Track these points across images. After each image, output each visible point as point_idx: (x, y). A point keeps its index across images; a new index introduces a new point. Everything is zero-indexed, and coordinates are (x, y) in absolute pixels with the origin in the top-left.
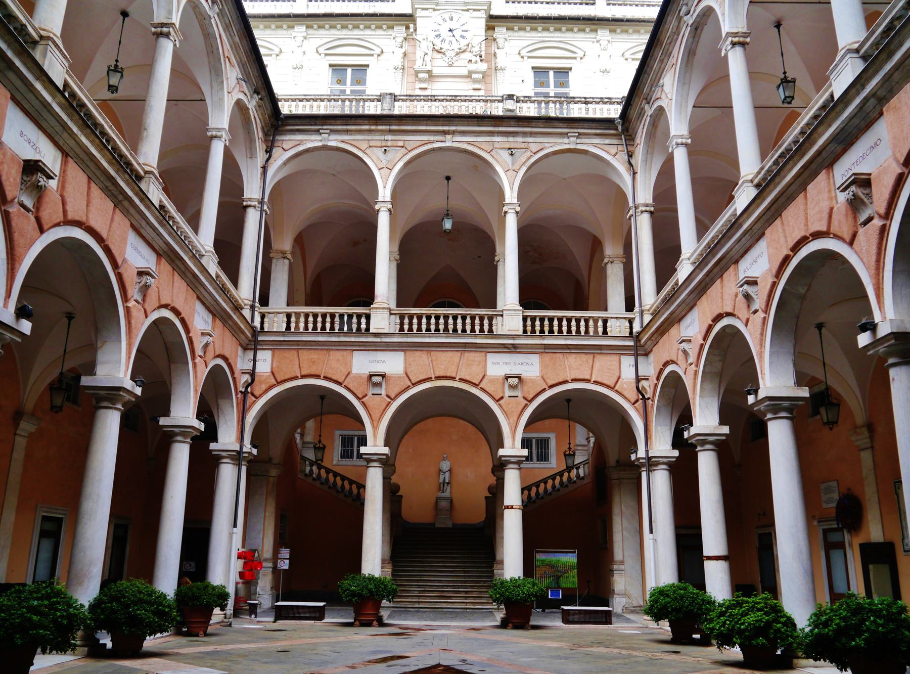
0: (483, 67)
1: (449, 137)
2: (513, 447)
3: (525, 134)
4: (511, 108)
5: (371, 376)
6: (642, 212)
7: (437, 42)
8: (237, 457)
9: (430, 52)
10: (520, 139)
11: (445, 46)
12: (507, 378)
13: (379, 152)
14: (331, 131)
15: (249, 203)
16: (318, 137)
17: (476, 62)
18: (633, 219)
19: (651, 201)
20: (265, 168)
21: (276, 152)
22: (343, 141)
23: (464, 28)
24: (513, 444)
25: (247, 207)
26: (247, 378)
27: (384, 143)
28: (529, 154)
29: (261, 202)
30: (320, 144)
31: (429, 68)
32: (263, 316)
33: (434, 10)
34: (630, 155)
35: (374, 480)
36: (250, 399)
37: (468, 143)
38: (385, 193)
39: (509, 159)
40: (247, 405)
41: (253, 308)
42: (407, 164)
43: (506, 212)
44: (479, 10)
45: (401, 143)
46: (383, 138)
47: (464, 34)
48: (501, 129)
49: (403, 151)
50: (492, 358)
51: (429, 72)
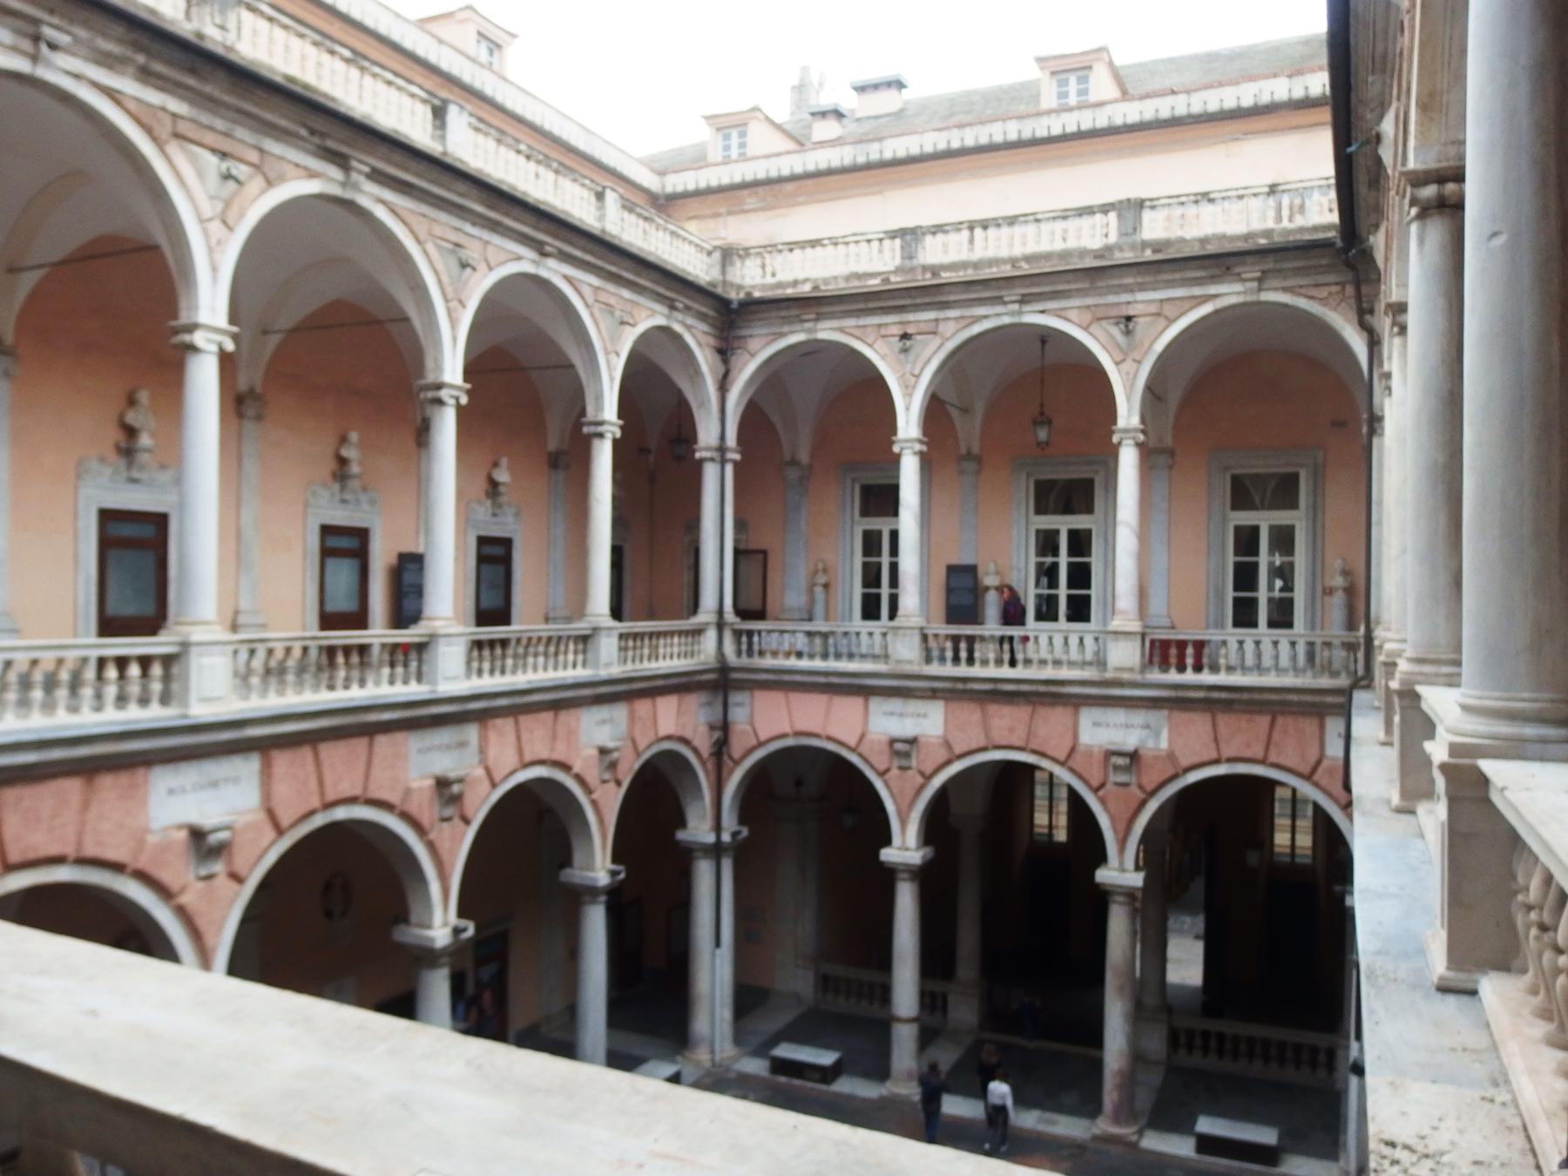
2: (1123, 870)
5: (893, 741)
8: (716, 851)
12: (1110, 753)
20: (723, 388)
24: (1121, 863)
25: (702, 461)
26: (717, 734)
29: (722, 449)
32: (738, 634)
35: (906, 902)
36: (728, 762)
40: (725, 774)
41: (720, 626)
43: (1120, 443)
50: (1087, 717)
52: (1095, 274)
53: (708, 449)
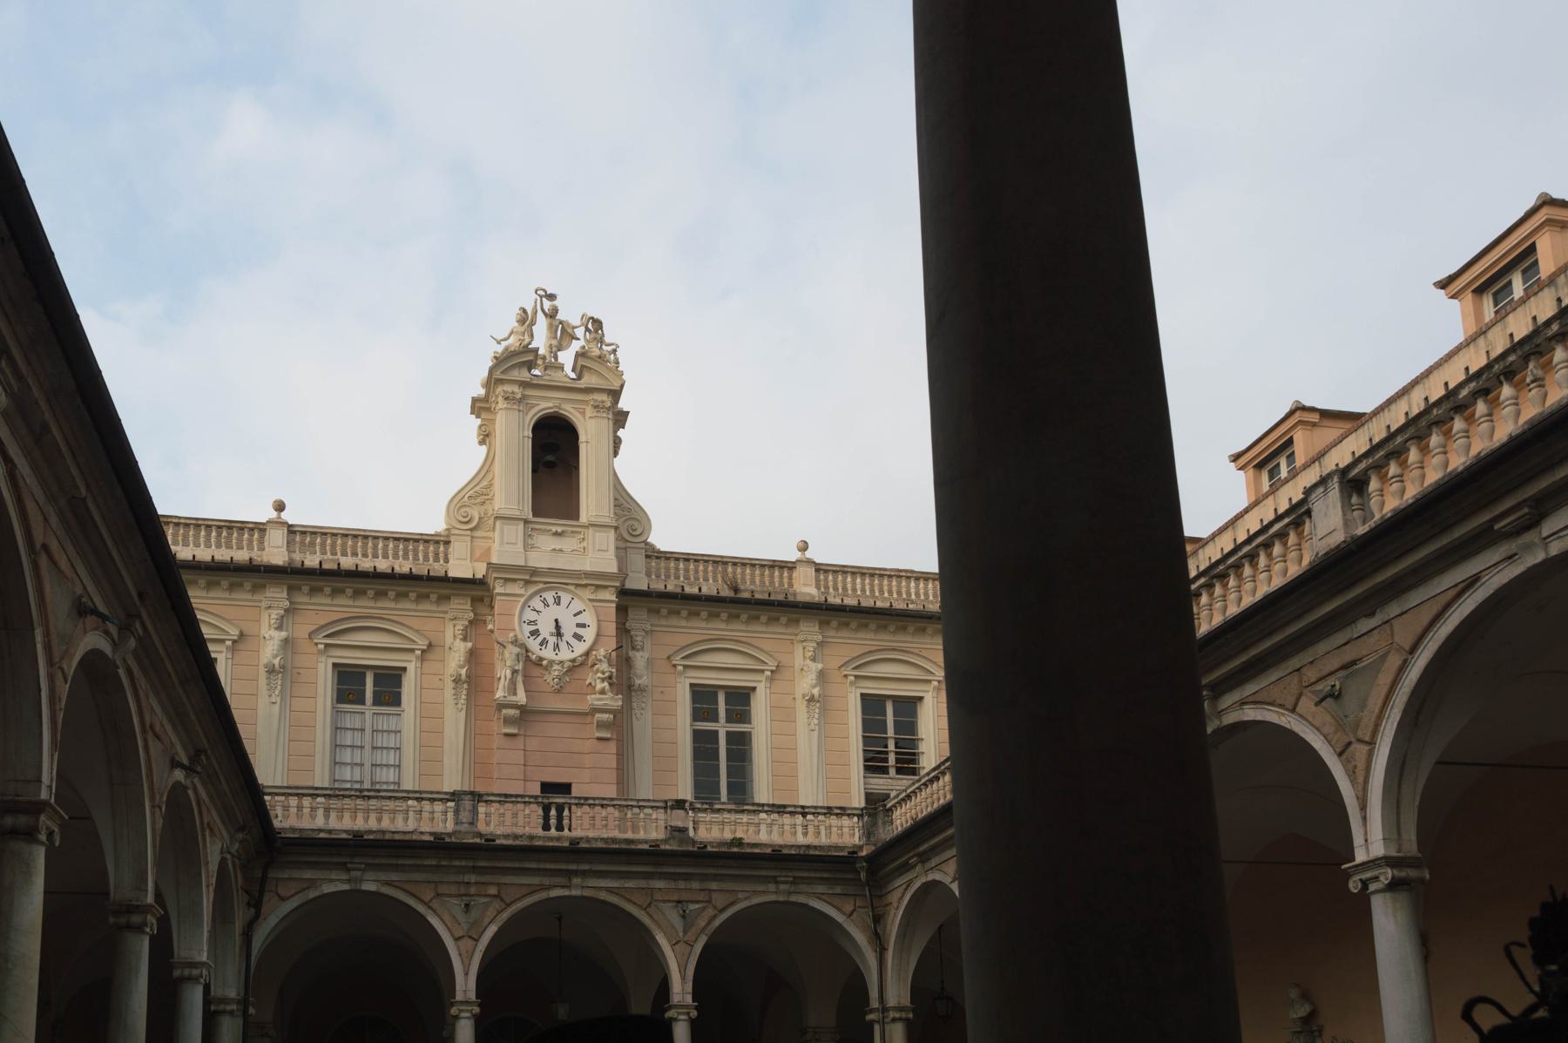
0: (615, 702)
1: (576, 881)
3: (705, 878)
4: (680, 824)
6: (894, 1020)
7: (533, 644)
9: (520, 667)
10: (695, 885)
11: (548, 653)
13: (456, 905)
14: (367, 865)
15: (222, 1007)
16: (345, 877)
17: (603, 692)
18: (877, 1027)
19: (906, 1001)
21: (269, 900)
22: (388, 883)
23: (580, 619)
27: (463, 891)
28: (710, 912)
30: (346, 887)
31: (521, 697)
33: (527, 583)
34: (878, 919)
37: (610, 890)
38: (465, 985)
39: (678, 924)
42: (501, 930)
44: (606, 587)
45: (493, 890)
46: (460, 878)
47: (580, 631)
48: (666, 869)
49: (497, 905)
51: (521, 708)
52: (651, 859)
53: (225, 1001)
